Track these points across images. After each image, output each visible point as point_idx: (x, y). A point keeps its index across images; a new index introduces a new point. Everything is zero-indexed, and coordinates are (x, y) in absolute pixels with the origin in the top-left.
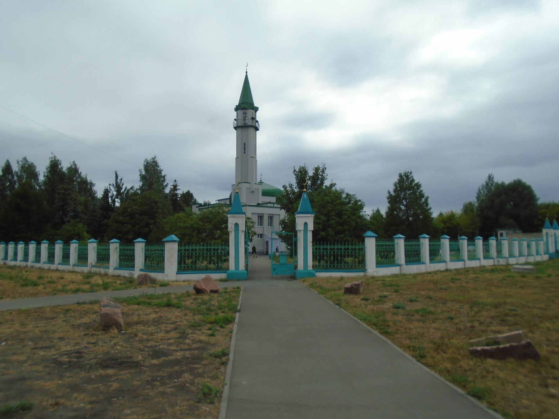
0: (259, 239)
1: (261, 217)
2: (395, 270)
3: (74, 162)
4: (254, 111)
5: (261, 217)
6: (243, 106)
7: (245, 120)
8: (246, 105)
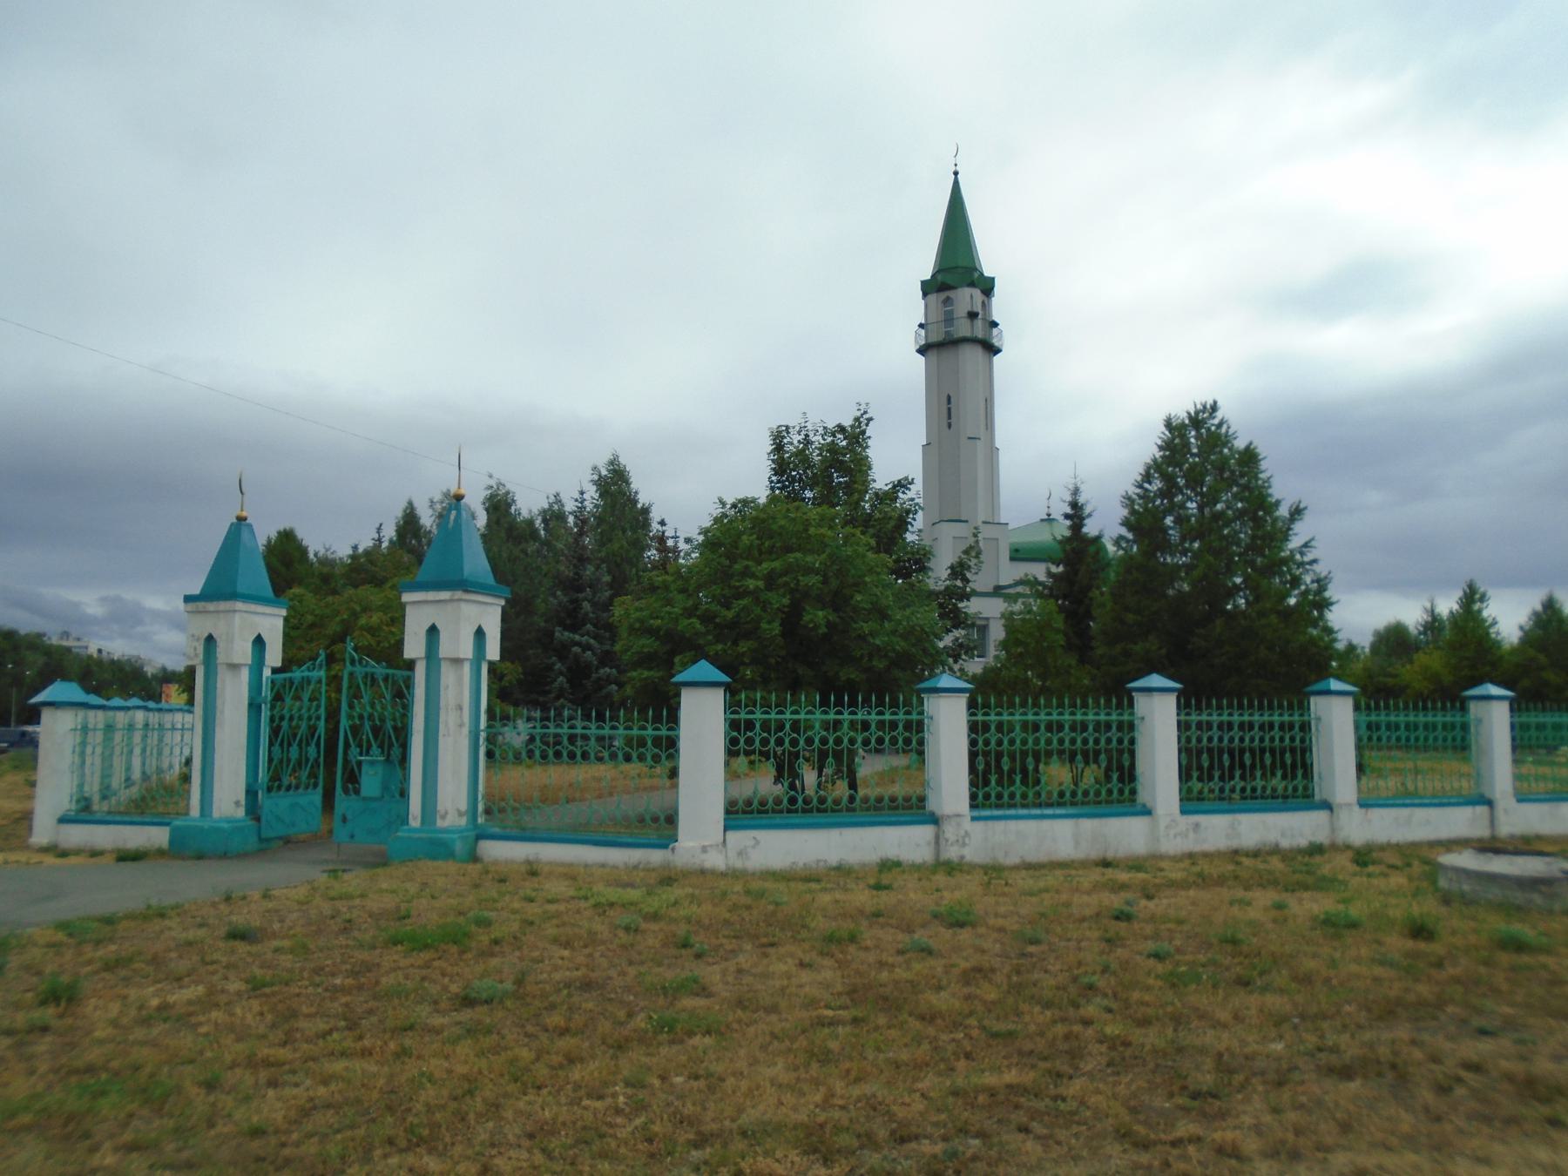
2: (904, 842)
3: (557, 495)
4: (977, 293)
7: (949, 319)
8: (957, 275)
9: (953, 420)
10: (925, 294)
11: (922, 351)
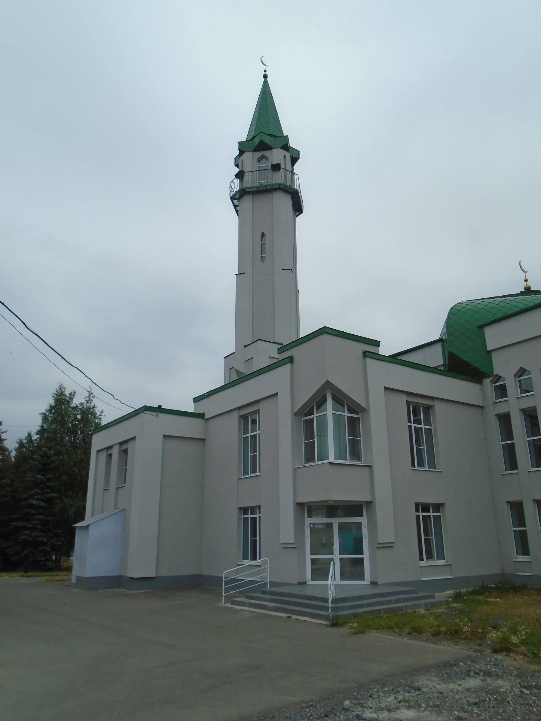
6: (257, 140)
9: (267, 254)
10: (241, 152)
11: (237, 198)
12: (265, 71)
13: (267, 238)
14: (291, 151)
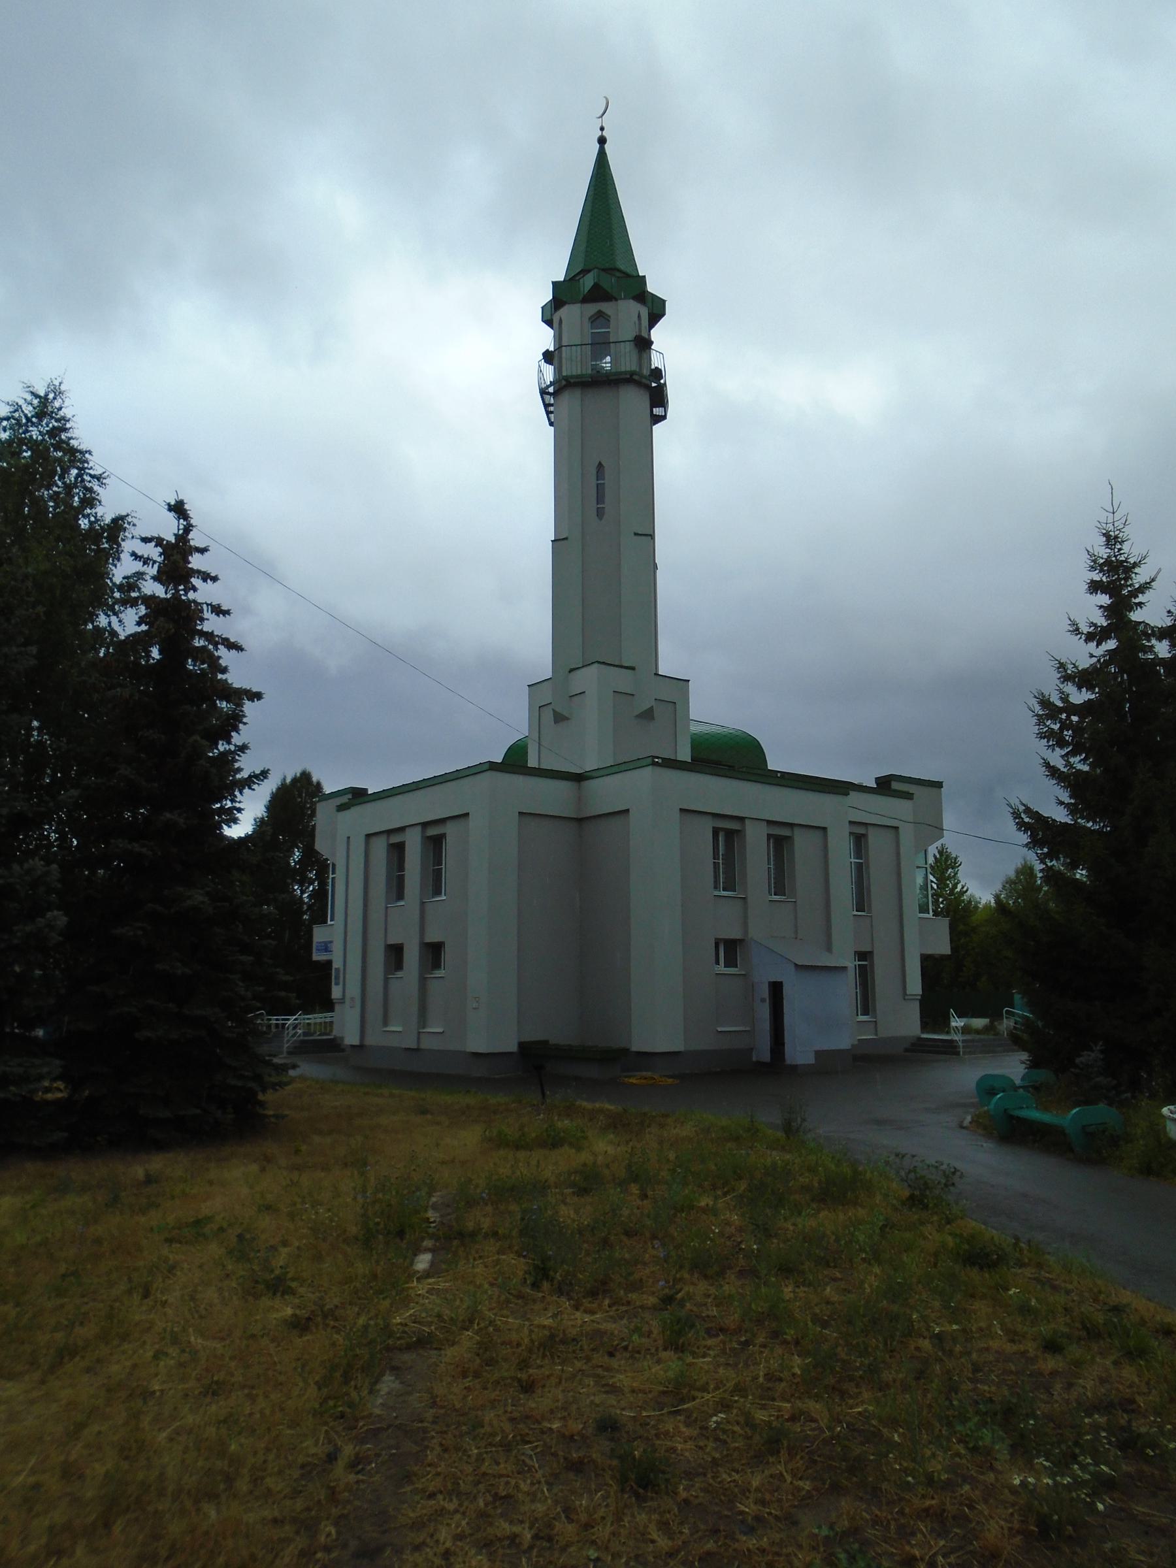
0: (721, 968)
1: (728, 834)
5: (728, 834)
6: (588, 282)
12: (602, 129)
13: (607, 473)
14: (650, 304)
